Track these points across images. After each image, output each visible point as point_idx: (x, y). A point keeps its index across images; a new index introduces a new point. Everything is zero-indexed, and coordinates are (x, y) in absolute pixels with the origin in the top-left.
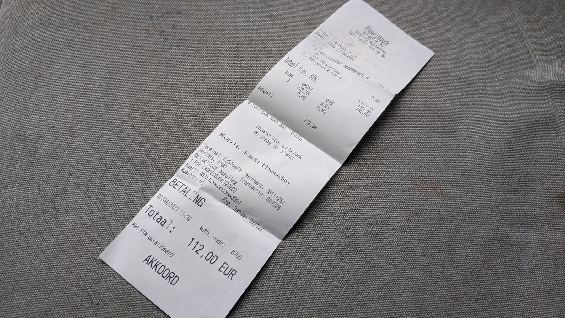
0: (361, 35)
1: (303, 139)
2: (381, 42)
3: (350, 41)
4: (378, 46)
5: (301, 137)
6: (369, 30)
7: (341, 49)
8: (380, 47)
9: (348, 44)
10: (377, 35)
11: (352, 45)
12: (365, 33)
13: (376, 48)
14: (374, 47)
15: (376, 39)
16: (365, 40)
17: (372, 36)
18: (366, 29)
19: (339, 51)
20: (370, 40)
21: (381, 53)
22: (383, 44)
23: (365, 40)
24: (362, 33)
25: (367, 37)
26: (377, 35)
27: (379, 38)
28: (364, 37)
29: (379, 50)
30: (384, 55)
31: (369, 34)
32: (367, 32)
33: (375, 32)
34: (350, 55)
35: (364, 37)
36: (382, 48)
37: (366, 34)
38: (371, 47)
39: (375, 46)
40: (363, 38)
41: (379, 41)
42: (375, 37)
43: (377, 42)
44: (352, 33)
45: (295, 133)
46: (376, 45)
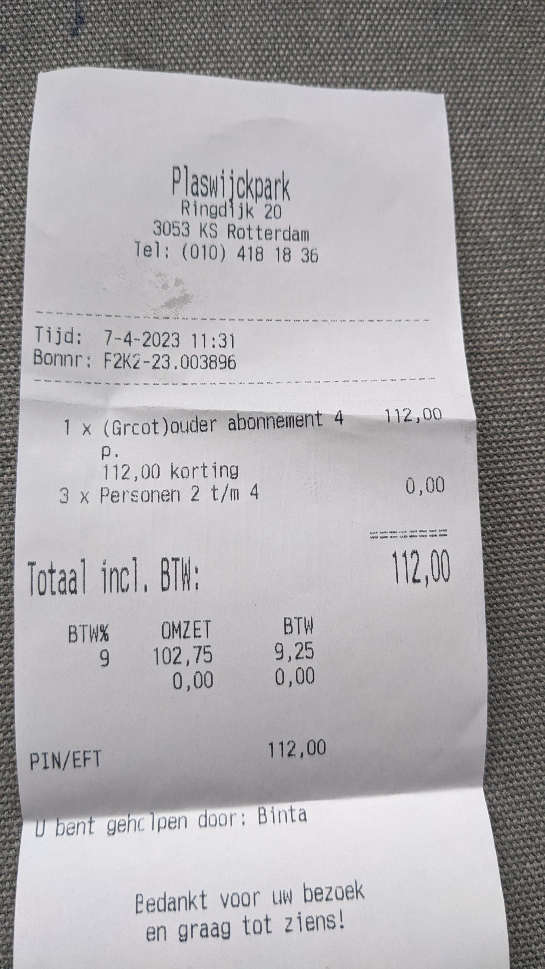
0: (183, 229)
1: (309, 806)
2: (262, 200)
3: (165, 287)
4: (265, 224)
5: (297, 806)
6: (191, 181)
7: (161, 351)
8: (272, 224)
9: (170, 304)
10: (228, 182)
11: (185, 299)
12: (185, 208)
13: (263, 243)
14: (255, 243)
15: (237, 201)
16: (208, 242)
17: (218, 200)
18: (180, 187)
19: (162, 362)
20: (222, 223)
21: (296, 247)
22: (273, 202)
23: (208, 242)
24: (175, 215)
25: (206, 219)
26: (228, 182)
27: (243, 188)
28: (195, 230)
29: (282, 244)
30: (309, 245)
31: (200, 200)
32: (191, 199)
33: (214, 173)
34: (209, 351)
35: (195, 230)
36: (281, 224)
37: (191, 209)
38: (247, 252)
39: (254, 233)
40: (195, 237)
41: (251, 201)
42: (228, 195)
43: (248, 212)
44: (147, 250)
45: (268, 808)
46: (254, 227)
